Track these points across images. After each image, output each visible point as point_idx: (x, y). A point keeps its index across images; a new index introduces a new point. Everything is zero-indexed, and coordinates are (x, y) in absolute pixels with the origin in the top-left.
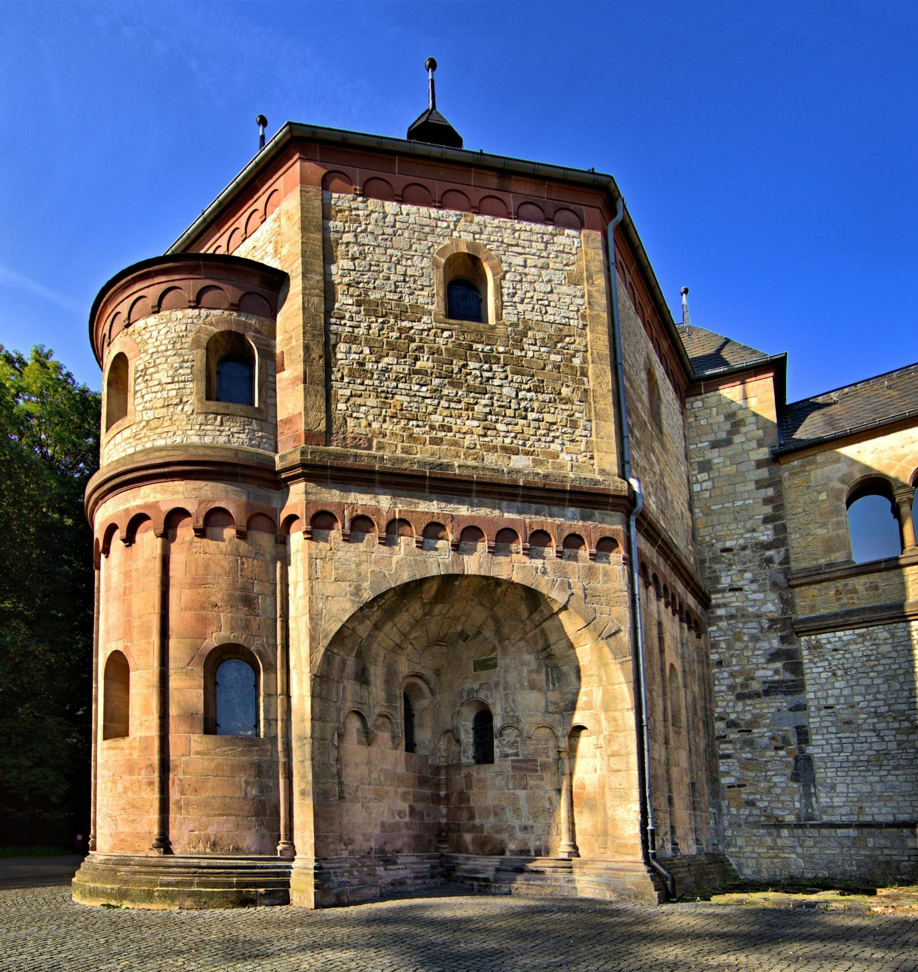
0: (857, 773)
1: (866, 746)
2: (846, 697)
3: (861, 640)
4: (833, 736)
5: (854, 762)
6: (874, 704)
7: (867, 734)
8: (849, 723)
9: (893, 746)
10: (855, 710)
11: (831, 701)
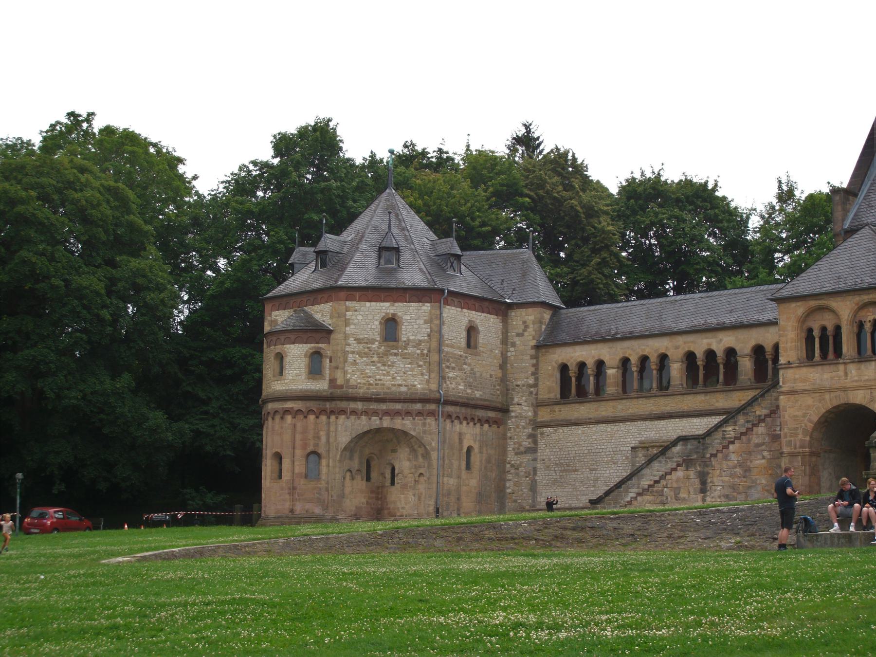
8: (548, 467)
9: (558, 477)
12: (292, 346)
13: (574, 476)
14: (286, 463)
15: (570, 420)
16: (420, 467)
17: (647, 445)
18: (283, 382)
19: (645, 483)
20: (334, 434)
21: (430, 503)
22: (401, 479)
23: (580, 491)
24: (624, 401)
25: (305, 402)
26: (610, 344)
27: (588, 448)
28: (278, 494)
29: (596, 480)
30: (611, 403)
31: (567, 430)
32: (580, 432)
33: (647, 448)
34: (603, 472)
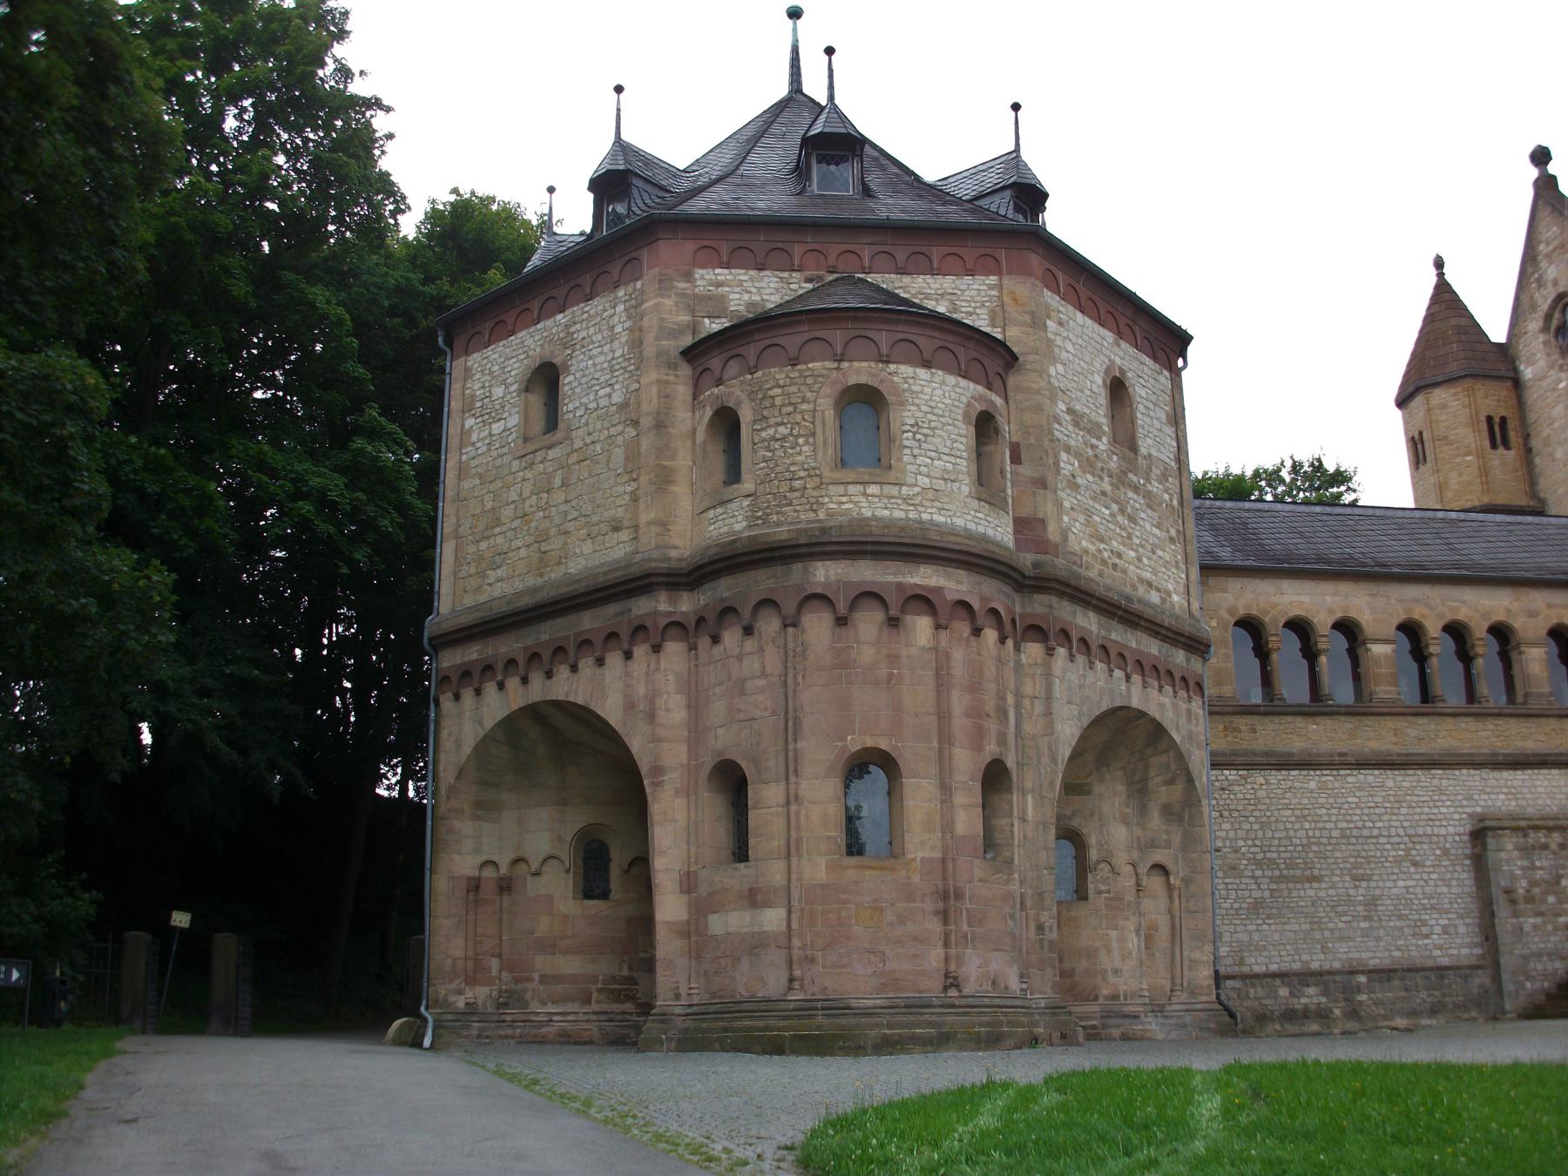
0: (1238, 922)
1: (1247, 893)
2: (1231, 840)
3: (1243, 782)
4: (1220, 881)
5: (1237, 910)
6: (1253, 850)
7: (1247, 881)
8: (1233, 868)
9: (1267, 894)
10: (1238, 855)
11: (1219, 844)
12: (922, 373)
13: (1311, 893)
14: (766, 797)
15: (1291, 755)
16: (1153, 844)
17: (1523, 824)
20: (1039, 707)
21: (1197, 955)
22: (1105, 881)
23: (1332, 930)
24: (1422, 720)
25: (981, 579)
26: (1372, 587)
27: (1341, 825)
28: (890, 916)
29: (1372, 903)
30: (1390, 723)
31: (1275, 777)
32: (1313, 785)
33: (1523, 831)
34: (1389, 884)
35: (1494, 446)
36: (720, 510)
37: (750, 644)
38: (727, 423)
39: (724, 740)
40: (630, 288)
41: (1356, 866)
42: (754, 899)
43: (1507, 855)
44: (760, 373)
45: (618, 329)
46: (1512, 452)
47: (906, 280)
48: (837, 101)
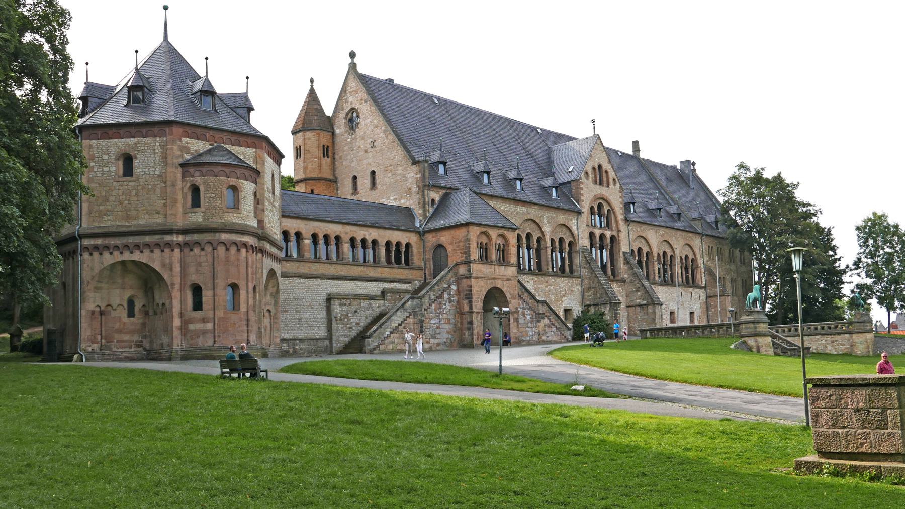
12: (246, 182)
13: (285, 315)
18: (239, 215)
19: (394, 325)
20: (260, 271)
24: (316, 264)
27: (294, 295)
29: (300, 319)
35: (324, 156)
36: (193, 214)
37: (203, 253)
38: (195, 190)
39: (194, 278)
40: (161, 139)
41: (297, 308)
42: (204, 320)
43: (336, 306)
44: (206, 178)
45: (157, 151)
46: (329, 159)
47: (234, 147)
48: (170, 40)
